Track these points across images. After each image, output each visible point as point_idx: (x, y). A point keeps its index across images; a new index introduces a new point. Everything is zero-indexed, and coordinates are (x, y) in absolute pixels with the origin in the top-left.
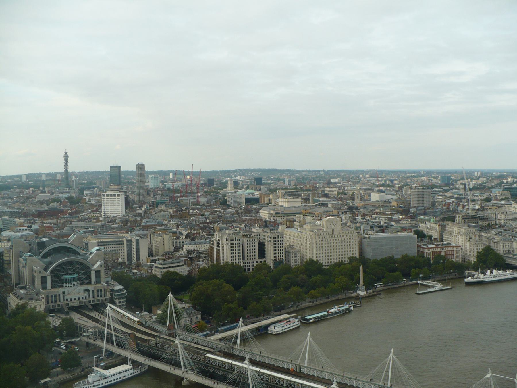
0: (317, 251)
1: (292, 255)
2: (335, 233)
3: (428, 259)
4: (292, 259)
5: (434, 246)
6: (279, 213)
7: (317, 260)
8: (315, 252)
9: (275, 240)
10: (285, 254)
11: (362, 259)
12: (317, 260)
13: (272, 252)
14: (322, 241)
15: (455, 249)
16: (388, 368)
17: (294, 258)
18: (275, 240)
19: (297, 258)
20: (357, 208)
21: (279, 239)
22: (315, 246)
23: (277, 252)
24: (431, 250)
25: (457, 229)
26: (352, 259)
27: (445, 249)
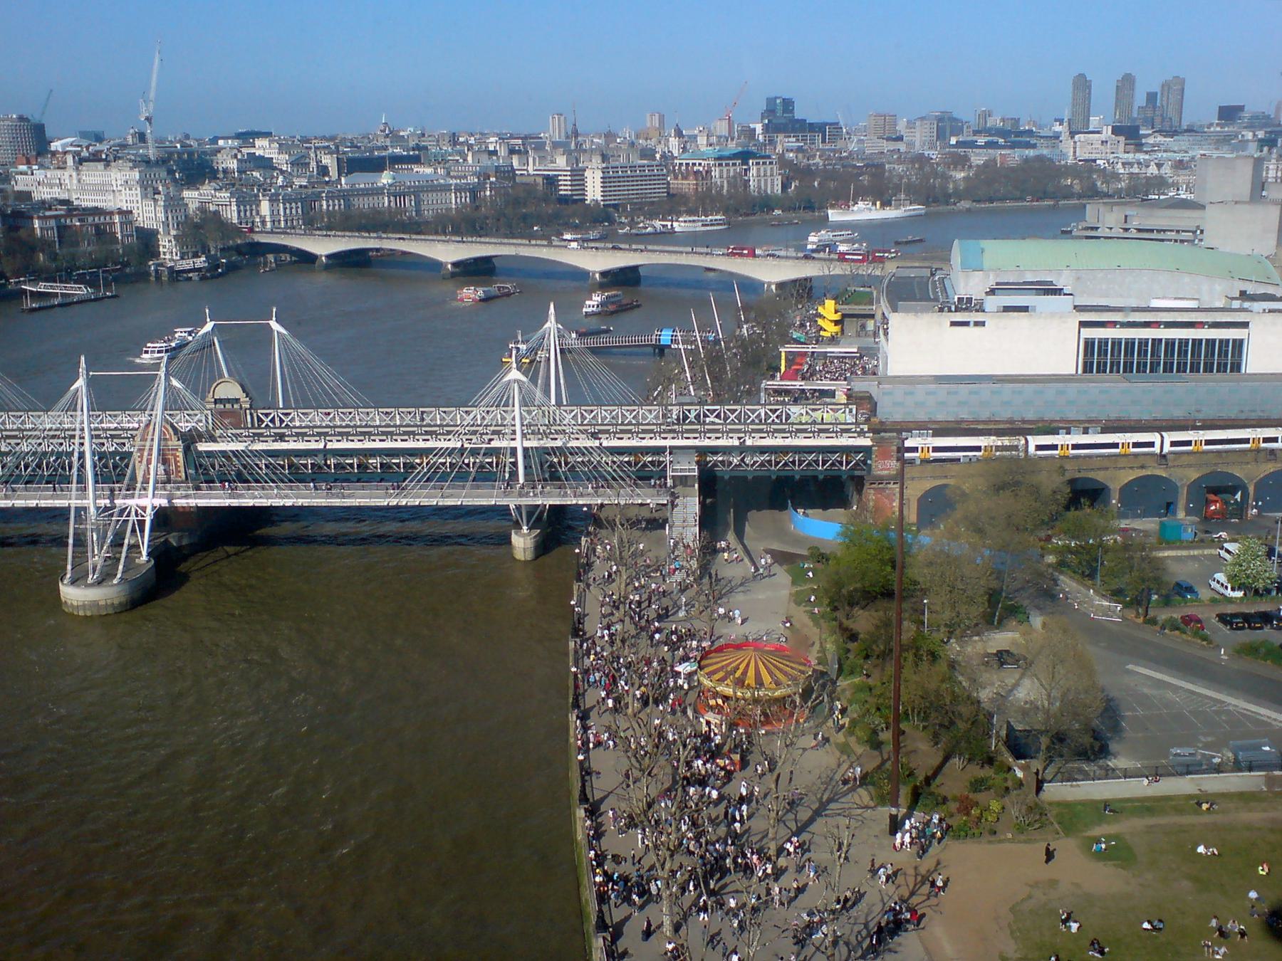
25: (119, 175)
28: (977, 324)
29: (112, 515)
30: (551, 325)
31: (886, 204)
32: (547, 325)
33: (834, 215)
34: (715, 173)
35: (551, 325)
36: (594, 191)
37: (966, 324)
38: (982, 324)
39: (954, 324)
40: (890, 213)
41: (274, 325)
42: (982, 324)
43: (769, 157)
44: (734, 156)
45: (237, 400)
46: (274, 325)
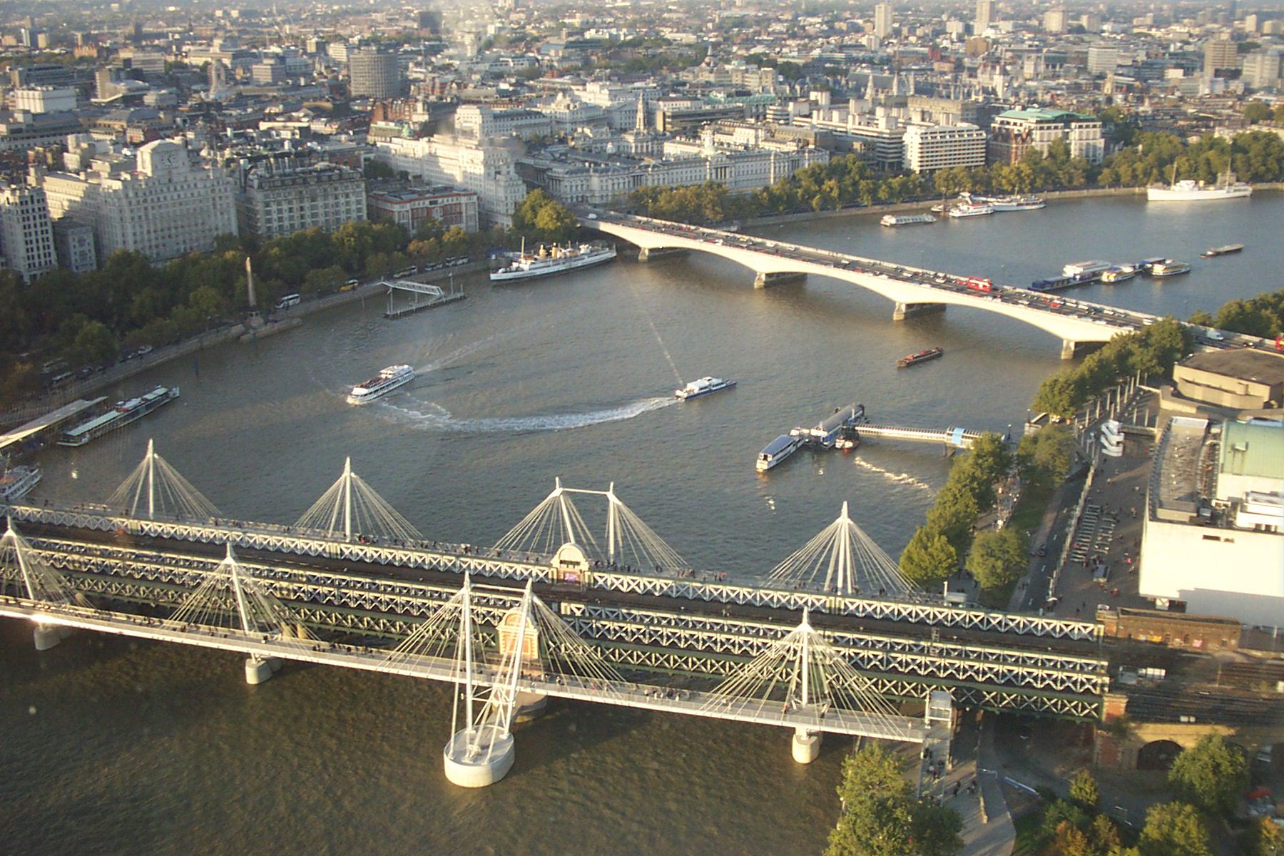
0: (134, 227)
1: (72, 242)
2: (175, 180)
3: (403, 228)
4: (72, 250)
5: (415, 196)
6: (20, 131)
7: (137, 251)
8: (130, 231)
9: (24, 208)
10: (55, 242)
11: (249, 240)
12: (137, 251)
13: (20, 238)
14: (145, 201)
15: (463, 200)
16: (342, 505)
17: (78, 250)
18: (24, 208)
19: (86, 248)
20: (217, 105)
21: (36, 206)
22: (127, 215)
23: (33, 238)
24: (408, 207)
26: (225, 241)
27: (440, 200)
28: (1227, 540)
29: (487, 696)
30: (843, 521)
31: (1211, 180)
32: (838, 521)
33: (1156, 194)
34: (1037, 135)
35: (843, 521)
36: (914, 160)
37: (1217, 538)
38: (1232, 541)
39: (1206, 537)
40: (1213, 194)
41: (611, 495)
42: (1232, 541)
43: (1093, 120)
44: (1055, 120)
45: (578, 563)
46: (611, 495)
